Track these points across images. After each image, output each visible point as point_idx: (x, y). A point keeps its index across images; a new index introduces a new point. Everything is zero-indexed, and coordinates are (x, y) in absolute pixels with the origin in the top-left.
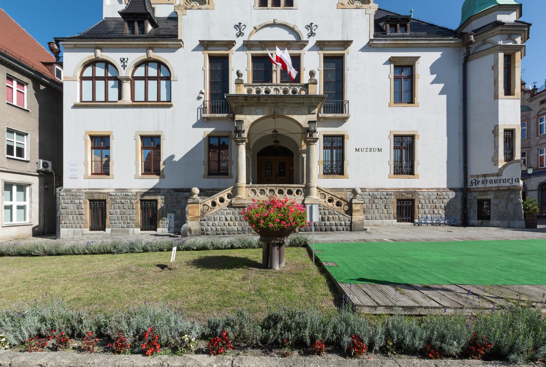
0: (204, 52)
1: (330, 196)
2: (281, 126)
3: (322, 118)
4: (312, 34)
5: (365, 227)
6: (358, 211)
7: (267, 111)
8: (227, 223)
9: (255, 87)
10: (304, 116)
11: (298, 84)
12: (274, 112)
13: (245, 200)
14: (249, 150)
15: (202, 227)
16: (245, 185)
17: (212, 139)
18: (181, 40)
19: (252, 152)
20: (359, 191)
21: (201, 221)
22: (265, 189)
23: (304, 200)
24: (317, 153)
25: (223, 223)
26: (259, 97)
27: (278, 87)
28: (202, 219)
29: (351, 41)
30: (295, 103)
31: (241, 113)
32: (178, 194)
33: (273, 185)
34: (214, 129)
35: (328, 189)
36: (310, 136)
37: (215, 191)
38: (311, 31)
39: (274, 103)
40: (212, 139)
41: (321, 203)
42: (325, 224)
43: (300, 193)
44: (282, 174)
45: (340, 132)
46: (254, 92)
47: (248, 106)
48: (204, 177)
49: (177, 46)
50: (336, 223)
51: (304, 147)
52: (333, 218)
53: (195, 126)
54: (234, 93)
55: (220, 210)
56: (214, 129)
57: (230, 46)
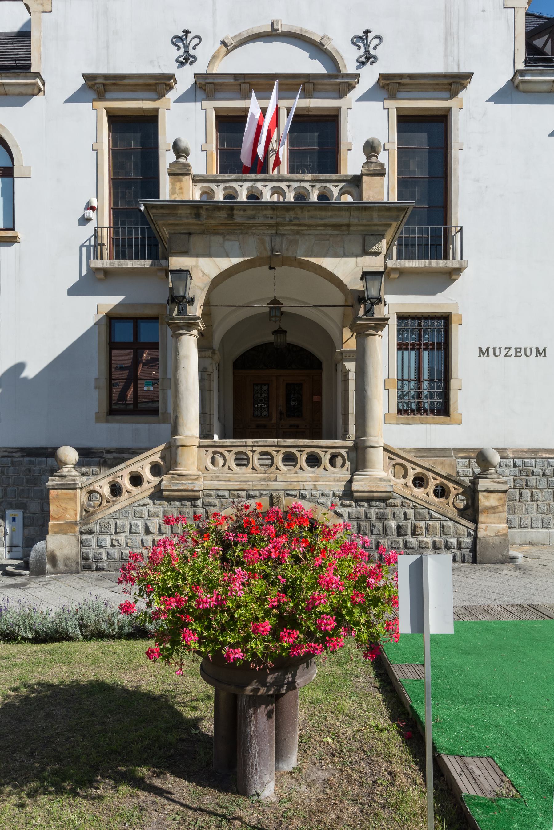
0: (95, 103)
1: (419, 470)
2: (292, 290)
3: (394, 269)
4: (368, 58)
5: (512, 553)
6: (493, 510)
7: (253, 248)
9: (223, 185)
10: (351, 262)
11: (334, 177)
12: (272, 250)
13: (196, 479)
14: (209, 353)
15: (85, 550)
16: (196, 441)
17: (118, 326)
18: (37, 75)
19: (217, 357)
20: (496, 458)
21: (81, 533)
22: (247, 450)
23: (351, 481)
25: (139, 539)
26: (232, 209)
27: (283, 185)
28: (84, 528)
29: (469, 76)
30: (326, 226)
31: (185, 253)
32: (31, 463)
33: (270, 441)
34: (122, 297)
35: (410, 451)
36: (366, 312)
37: (125, 456)
38: (367, 51)
39: (270, 226)
40: (118, 326)
41: (395, 488)
42: (406, 544)
43: (339, 461)
44: (293, 412)
45: (439, 305)
46: (219, 196)
47: (202, 233)
48: (98, 419)
49: (29, 90)
50: (434, 543)
51: (351, 344)
52: (427, 528)
53: (73, 291)
54: (168, 198)
55: (131, 505)
56: (122, 297)
57: (160, 88)
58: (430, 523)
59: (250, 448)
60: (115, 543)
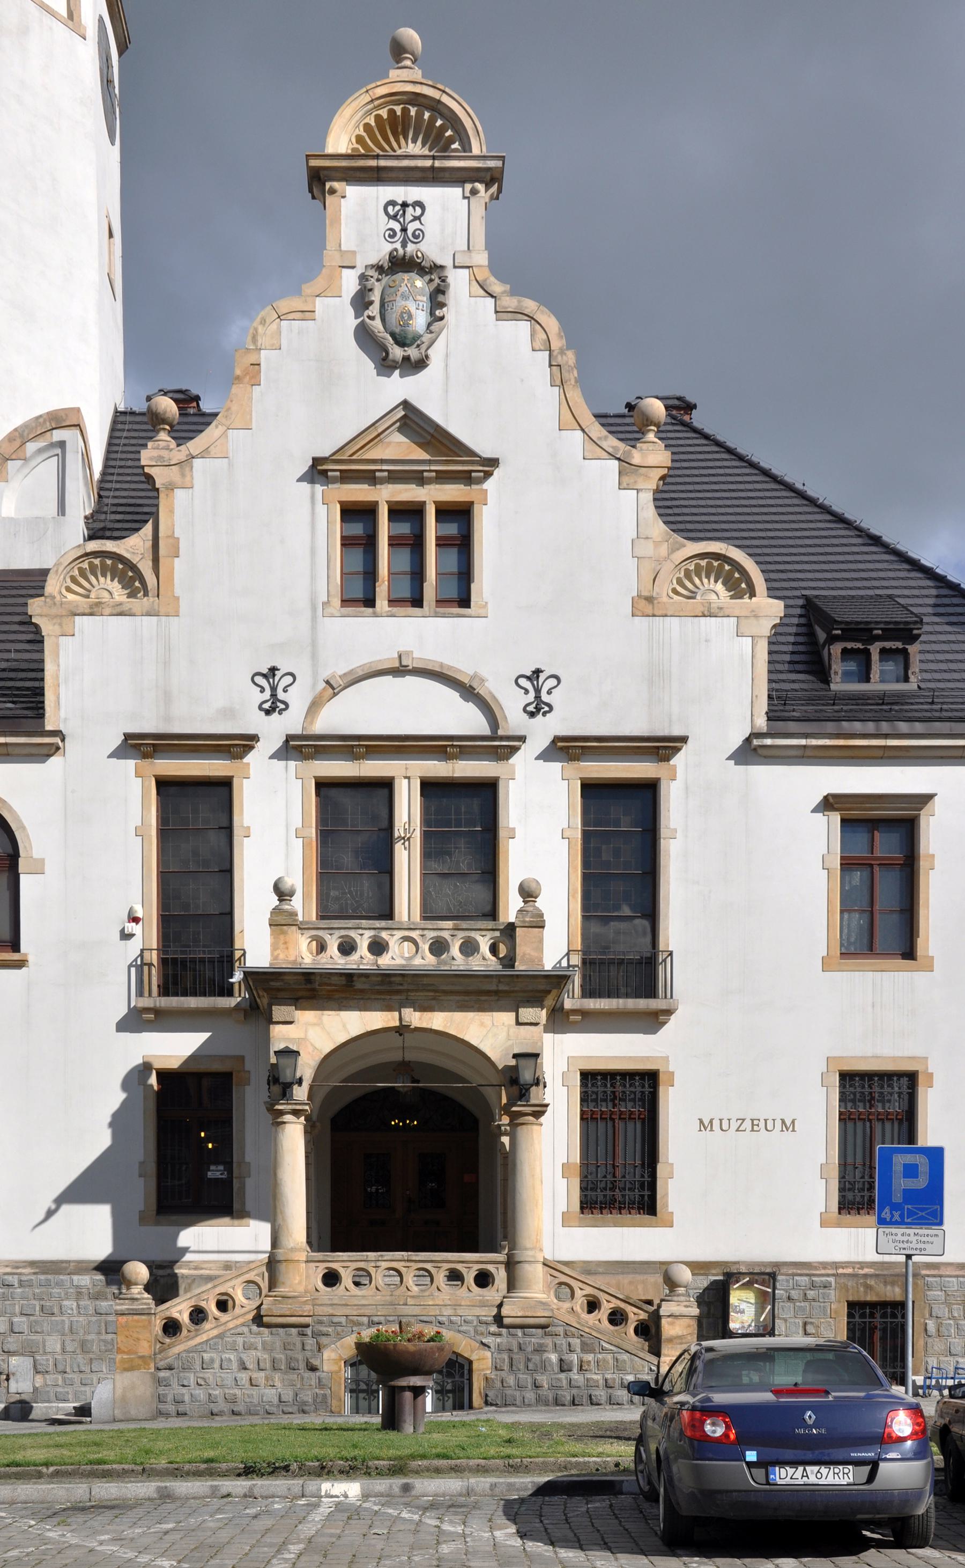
8: (244, 1377)
15: (161, 1390)
24: (549, 1152)
27: (415, 934)
55: (221, 1336)
58: (600, 1356)
59: (373, 1264)
60: (200, 1381)
